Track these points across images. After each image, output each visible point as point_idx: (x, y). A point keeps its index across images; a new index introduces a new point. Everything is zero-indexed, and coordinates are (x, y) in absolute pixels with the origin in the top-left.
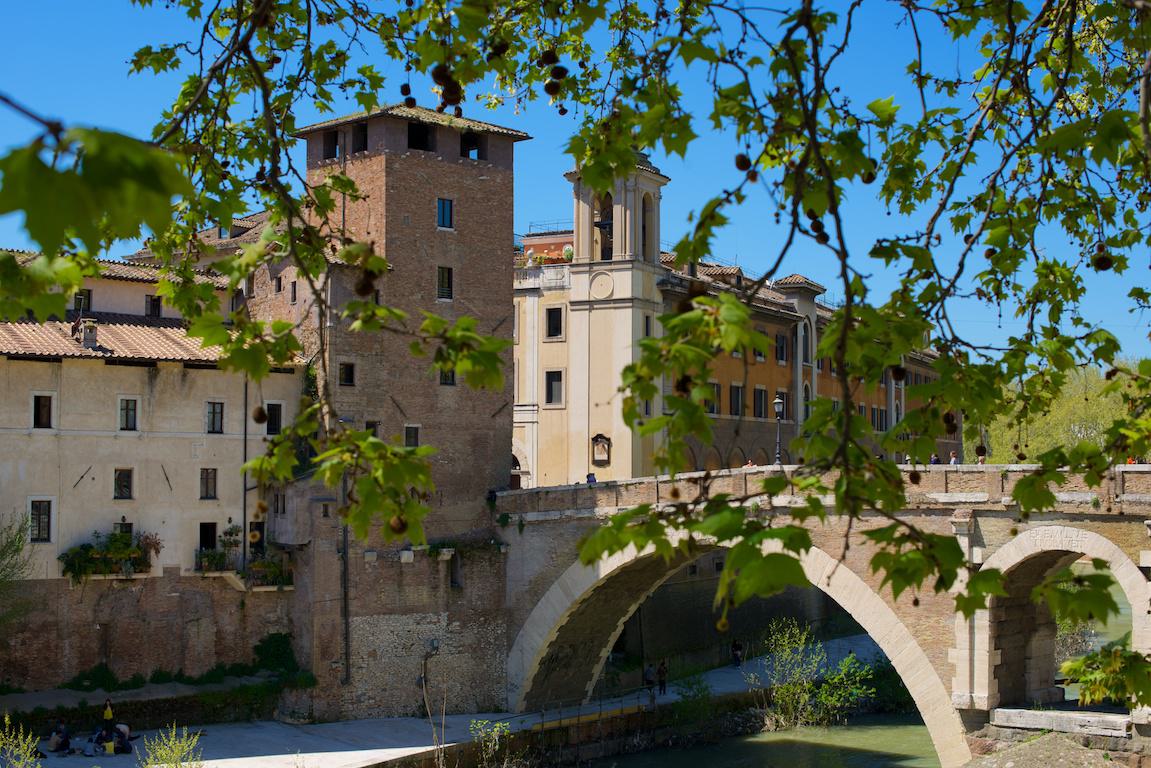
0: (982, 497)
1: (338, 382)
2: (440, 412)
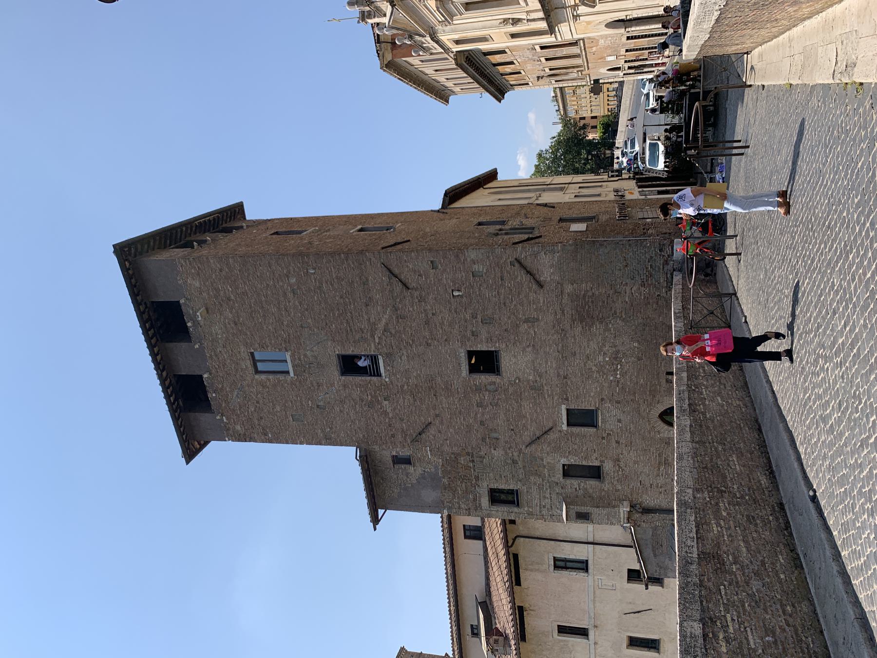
1: (516, 510)
2: (540, 376)
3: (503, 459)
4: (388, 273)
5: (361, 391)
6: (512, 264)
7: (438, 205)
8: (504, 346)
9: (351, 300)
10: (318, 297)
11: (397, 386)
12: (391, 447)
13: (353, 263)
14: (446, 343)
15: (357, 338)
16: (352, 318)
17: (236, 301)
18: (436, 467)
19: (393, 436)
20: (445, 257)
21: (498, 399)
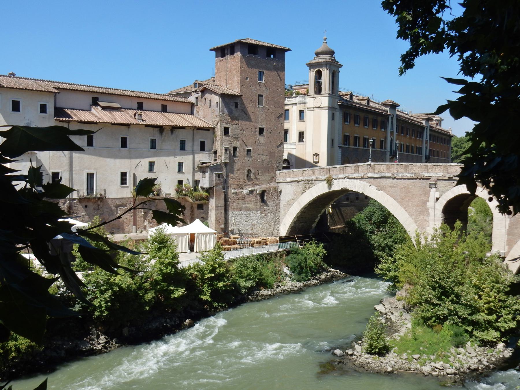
0: (441, 174)
18: (235, 114)
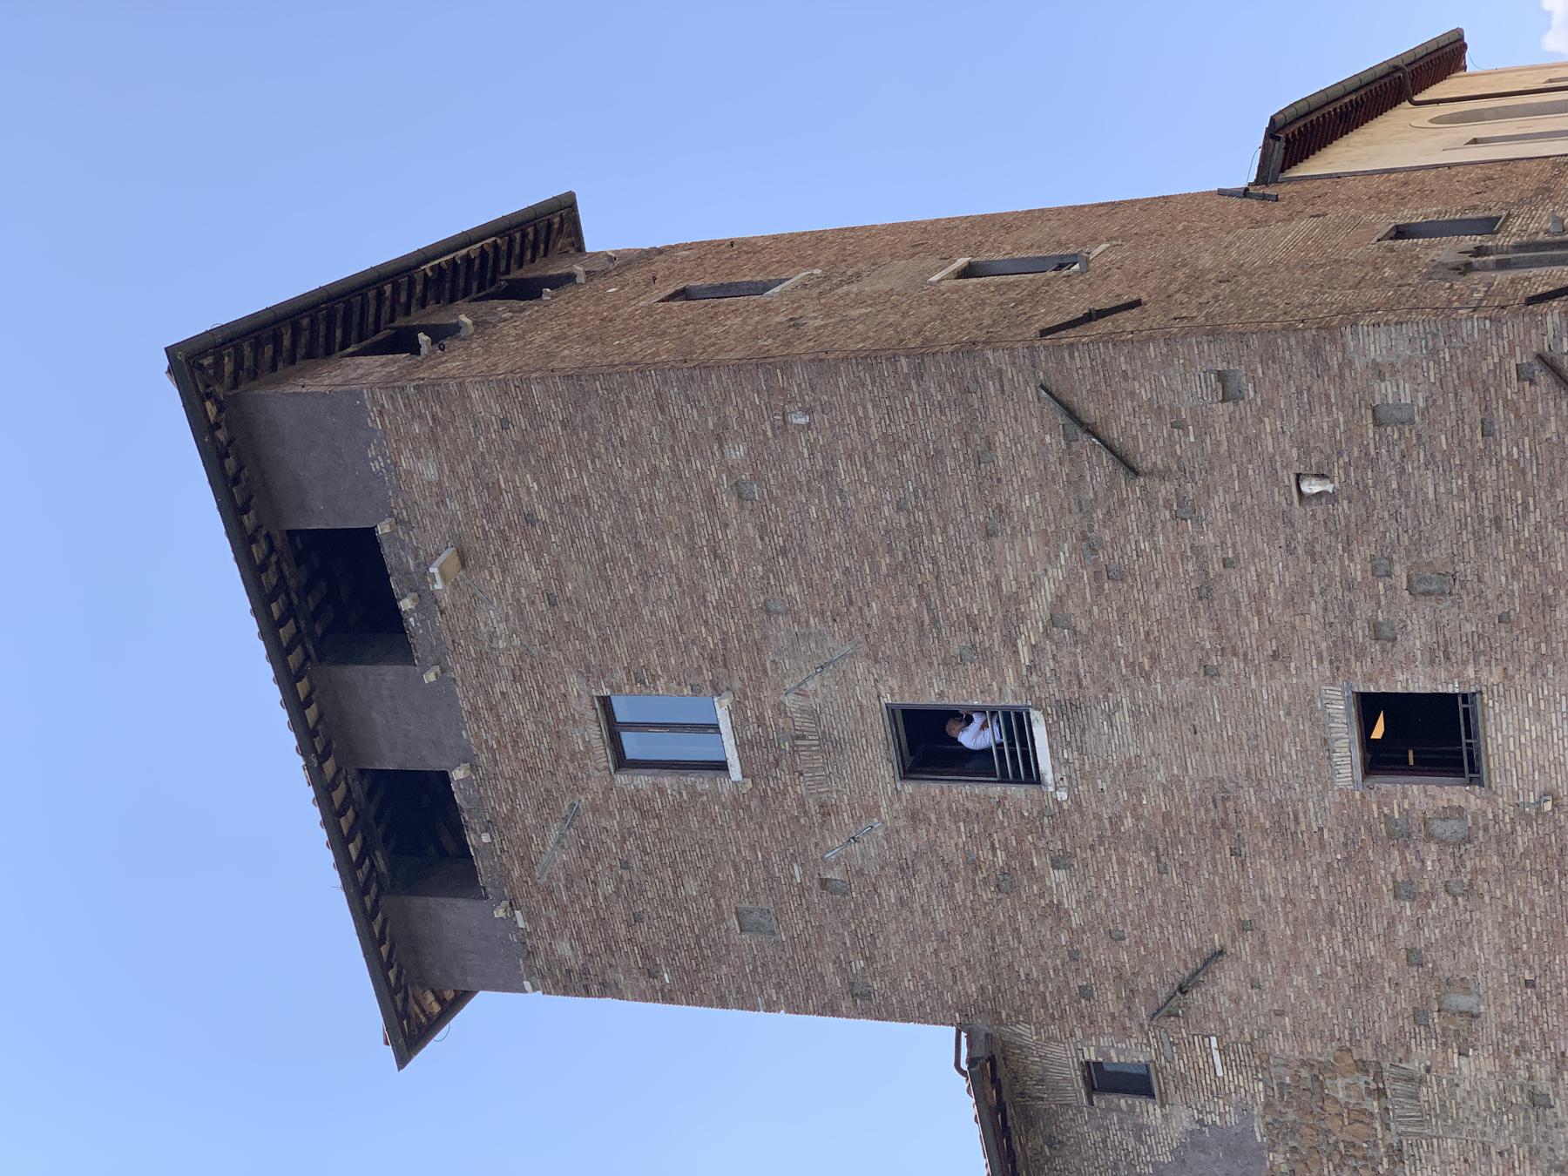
3: (1493, 1088)
4: (1062, 419)
5: (970, 835)
6: (1524, 374)
7: (1244, 173)
8: (1496, 679)
9: (933, 517)
10: (820, 510)
11: (1097, 816)
12: (1078, 1033)
13: (941, 388)
14: (1276, 665)
15: (955, 649)
16: (937, 578)
17: (554, 524)
18: (1244, 1110)
19: (1086, 993)
20: (1269, 358)
21: (1475, 871)
